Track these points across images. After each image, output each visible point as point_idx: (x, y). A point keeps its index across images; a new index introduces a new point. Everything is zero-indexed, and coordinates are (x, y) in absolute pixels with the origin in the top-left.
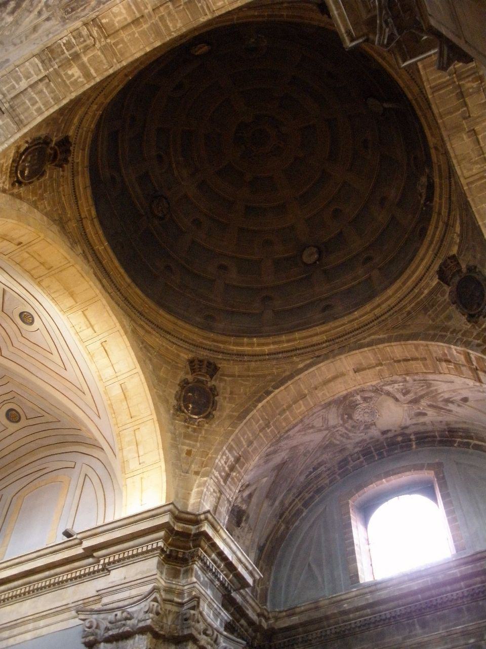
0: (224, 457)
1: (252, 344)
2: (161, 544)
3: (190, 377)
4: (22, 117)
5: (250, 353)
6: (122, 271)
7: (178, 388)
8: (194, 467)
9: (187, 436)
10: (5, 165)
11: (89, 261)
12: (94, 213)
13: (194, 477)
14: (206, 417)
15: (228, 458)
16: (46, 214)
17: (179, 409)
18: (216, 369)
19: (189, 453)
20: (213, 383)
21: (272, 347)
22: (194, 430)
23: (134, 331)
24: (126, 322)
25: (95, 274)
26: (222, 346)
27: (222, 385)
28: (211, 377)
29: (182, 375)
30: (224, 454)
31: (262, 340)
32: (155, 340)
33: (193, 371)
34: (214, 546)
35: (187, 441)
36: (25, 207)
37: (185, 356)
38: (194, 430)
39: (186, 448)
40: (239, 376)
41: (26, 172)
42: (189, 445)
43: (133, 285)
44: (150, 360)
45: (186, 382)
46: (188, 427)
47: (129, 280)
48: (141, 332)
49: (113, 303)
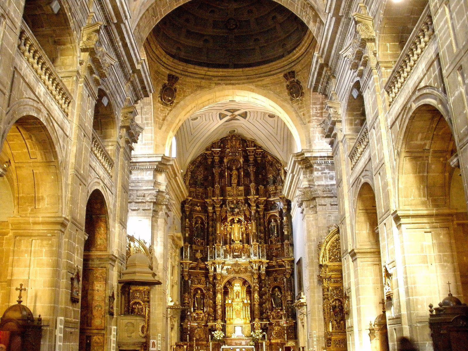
0: (314, 109)
1: (297, 52)
2: (300, 166)
3: (288, 83)
4: (148, 102)
5: (300, 55)
6: (235, 70)
7: (287, 91)
8: (307, 120)
9: (300, 108)
10: (162, 109)
11: (220, 84)
12: (206, 69)
13: (309, 124)
14: (301, 96)
15: (316, 108)
16: (192, 93)
17: (291, 100)
18: (293, 72)
19: (304, 115)
20: (296, 78)
21: (304, 48)
22: (301, 103)
23: (257, 86)
24: (251, 86)
25: (226, 85)
26: (290, 60)
27: (299, 77)
28: (294, 77)
29: (285, 84)
30: (313, 108)
31: (299, 48)
32: (267, 80)
33: (287, 79)
34: (316, 158)
35: (301, 110)
36: (182, 103)
37: (281, 75)
38: (301, 103)
39: (302, 113)
40: (302, 69)
41: (170, 99)
42: (302, 111)
43: (244, 69)
44: (270, 90)
45: (288, 86)
46: (299, 104)
47: (241, 70)
48: (259, 83)
49: (241, 86)
